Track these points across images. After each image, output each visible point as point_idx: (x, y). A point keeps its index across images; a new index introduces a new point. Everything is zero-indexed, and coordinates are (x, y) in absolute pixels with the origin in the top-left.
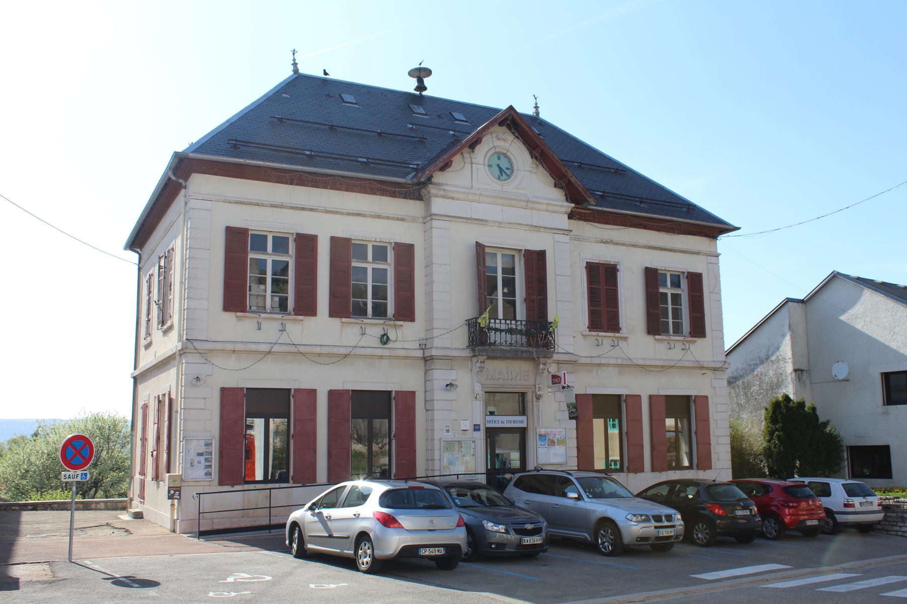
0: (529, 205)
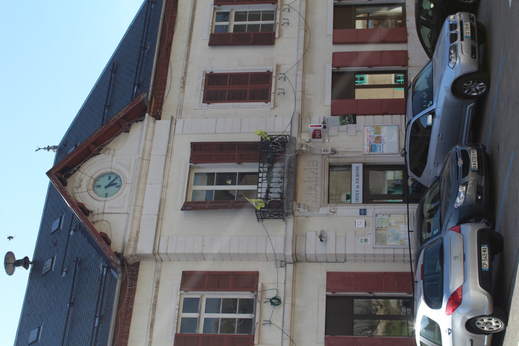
0: (146, 157)
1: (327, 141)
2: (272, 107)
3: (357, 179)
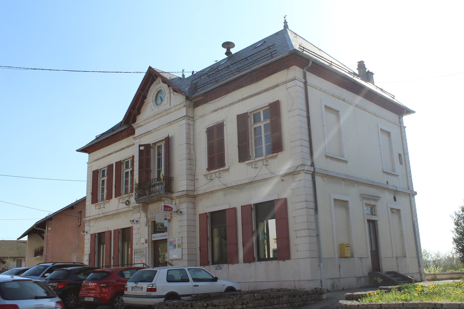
0: (168, 112)
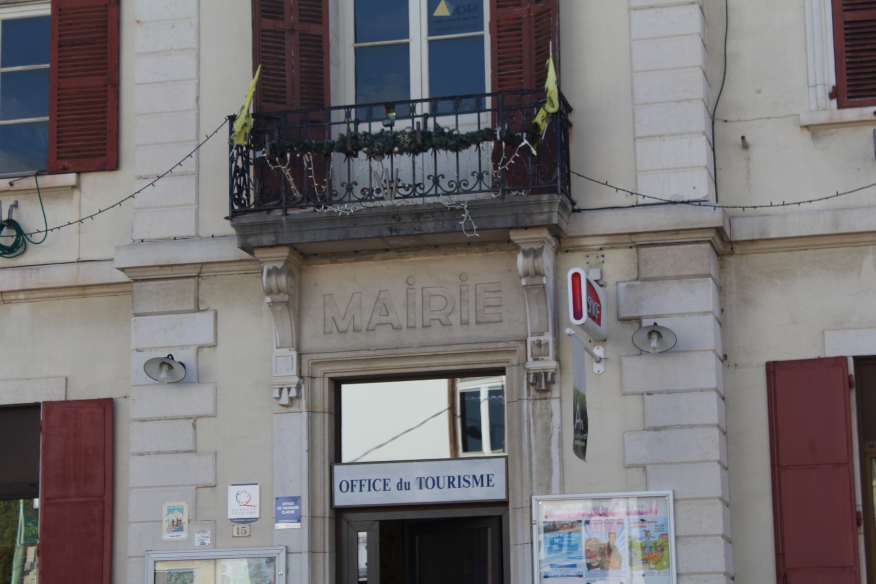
1: (599, 351)
2: (806, 120)
3: (436, 482)
